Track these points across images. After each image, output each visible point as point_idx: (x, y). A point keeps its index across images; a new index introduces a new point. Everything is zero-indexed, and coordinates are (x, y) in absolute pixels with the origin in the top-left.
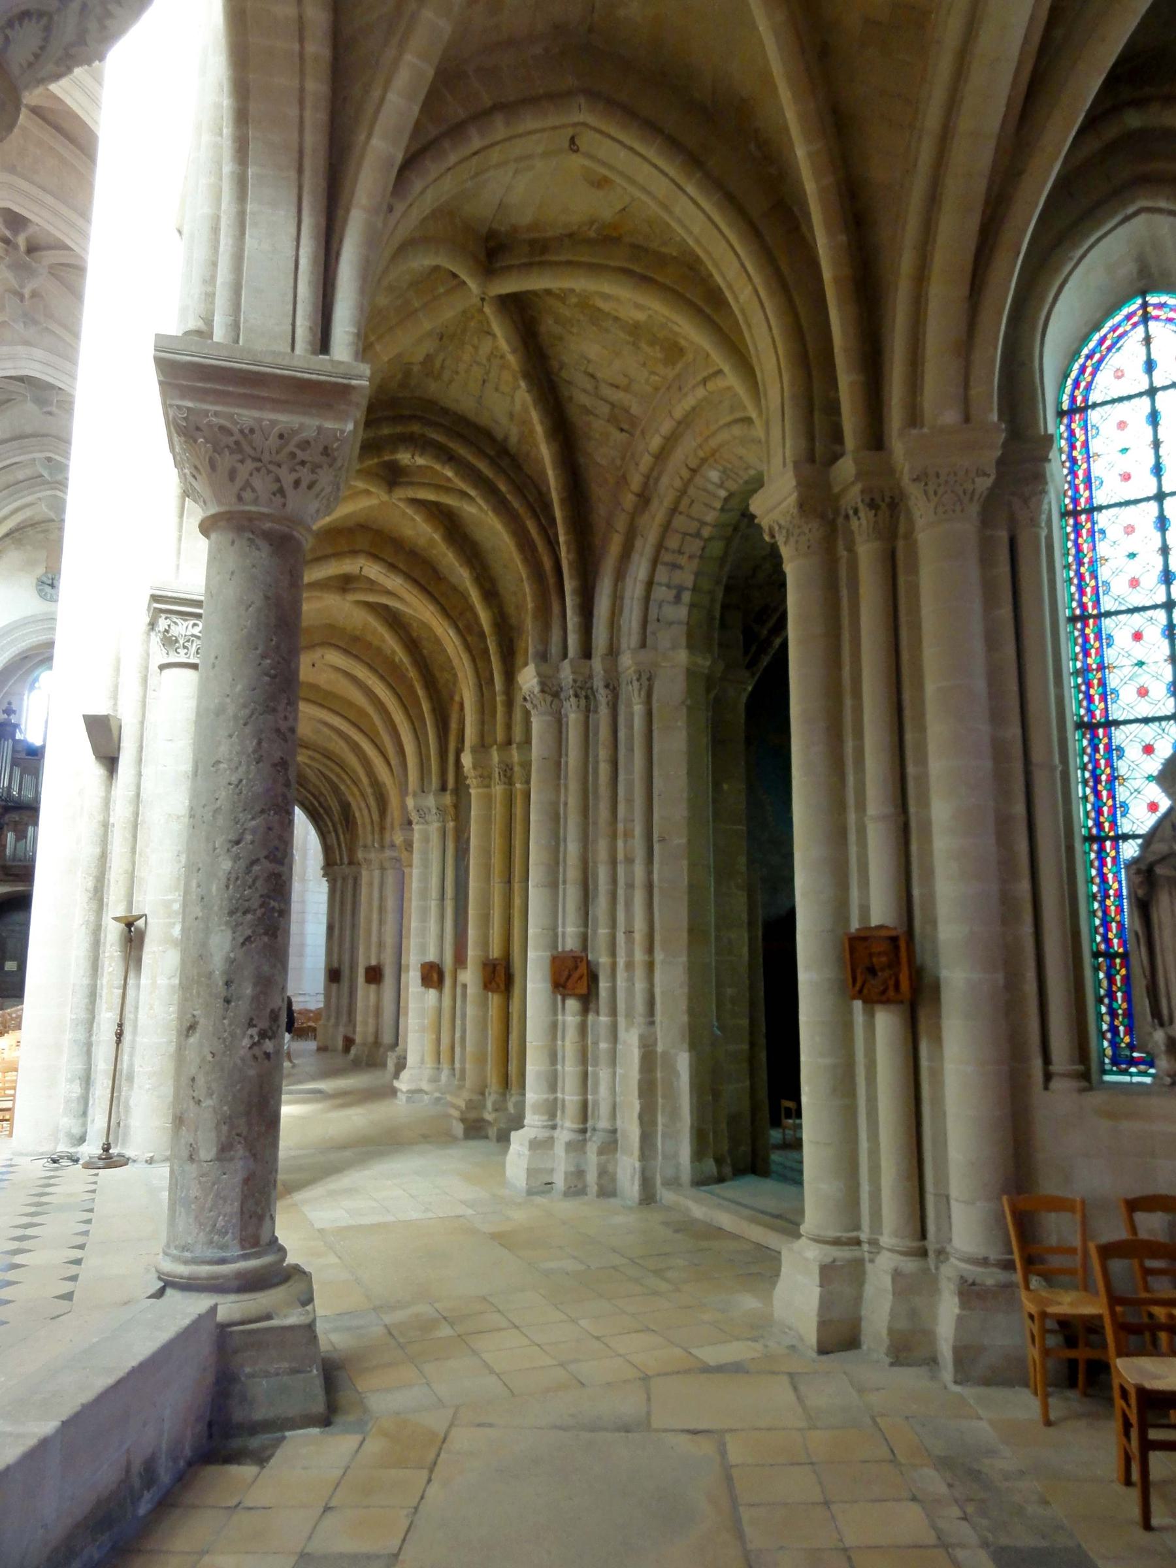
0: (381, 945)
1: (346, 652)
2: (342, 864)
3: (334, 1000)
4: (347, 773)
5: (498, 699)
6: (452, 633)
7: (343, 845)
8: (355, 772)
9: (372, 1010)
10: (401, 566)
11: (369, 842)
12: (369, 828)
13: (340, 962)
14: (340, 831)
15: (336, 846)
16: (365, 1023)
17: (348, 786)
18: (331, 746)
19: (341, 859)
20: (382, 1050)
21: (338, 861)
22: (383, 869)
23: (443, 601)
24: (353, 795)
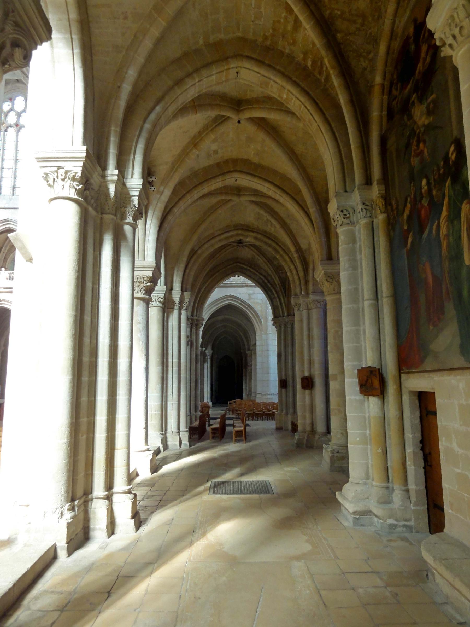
0: (311, 362)
2: (283, 316)
3: (284, 399)
4: (280, 246)
7: (283, 304)
8: (285, 245)
9: (308, 408)
12: (297, 283)
13: (286, 375)
15: (279, 305)
16: (304, 417)
18: (269, 228)
19: (283, 313)
20: (317, 437)
21: (281, 315)
22: (308, 309)
24: (285, 260)
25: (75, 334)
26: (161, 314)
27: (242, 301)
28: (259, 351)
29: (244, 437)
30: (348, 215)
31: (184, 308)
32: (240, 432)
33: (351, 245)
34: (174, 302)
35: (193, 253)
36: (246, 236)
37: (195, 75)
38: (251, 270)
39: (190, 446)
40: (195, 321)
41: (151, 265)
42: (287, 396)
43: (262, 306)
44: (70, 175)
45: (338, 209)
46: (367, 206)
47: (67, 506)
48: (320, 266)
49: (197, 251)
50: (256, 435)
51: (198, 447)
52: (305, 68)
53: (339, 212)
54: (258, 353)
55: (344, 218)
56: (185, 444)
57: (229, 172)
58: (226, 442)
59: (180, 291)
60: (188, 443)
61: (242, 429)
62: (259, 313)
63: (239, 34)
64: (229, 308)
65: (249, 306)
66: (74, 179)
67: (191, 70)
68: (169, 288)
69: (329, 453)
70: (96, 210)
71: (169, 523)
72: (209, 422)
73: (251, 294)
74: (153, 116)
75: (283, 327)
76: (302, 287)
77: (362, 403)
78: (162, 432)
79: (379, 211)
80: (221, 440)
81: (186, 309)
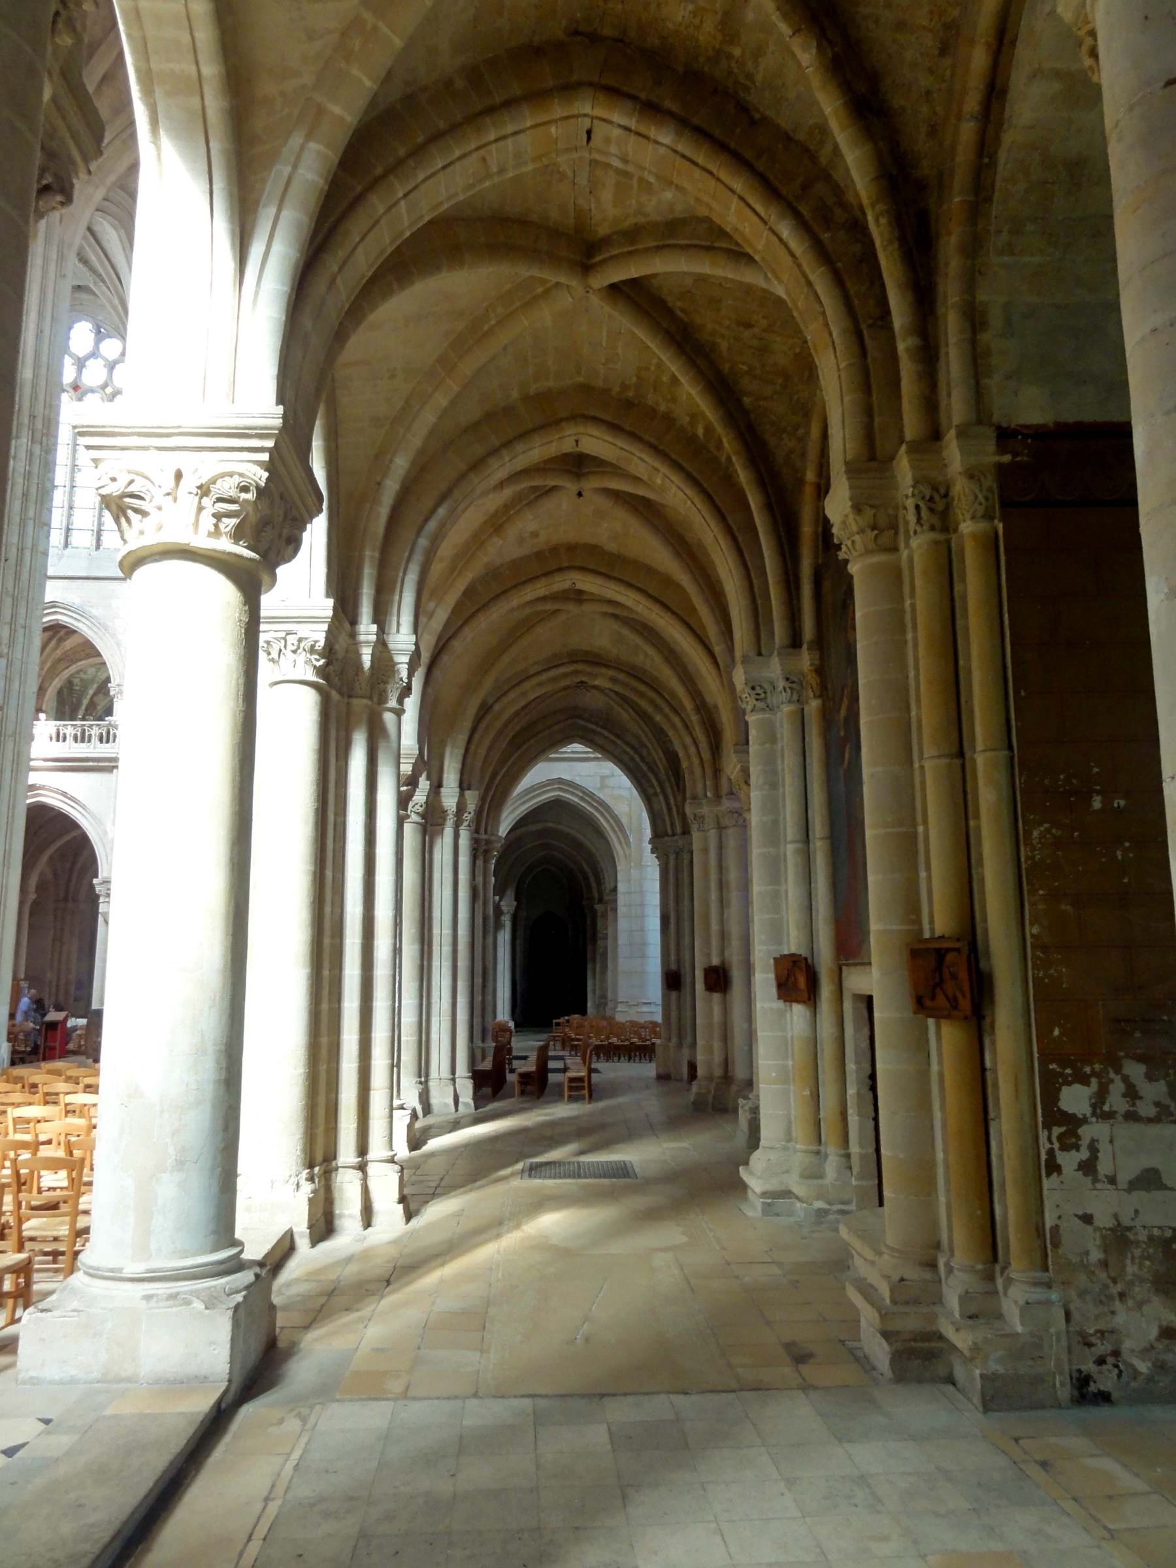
0: (724, 936)
1: (615, 428)
2: (674, 835)
3: (674, 1014)
5: (901, 347)
6: (786, 230)
7: (674, 810)
8: (673, 694)
9: (717, 1033)
10: (668, 104)
11: (700, 793)
12: (698, 771)
13: (679, 961)
14: (669, 791)
15: (665, 810)
16: (709, 1049)
17: (666, 716)
18: (639, 660)
19: (673, 825)
21: (670, 832)
22: (720, 828)
23: (760, 166)
25: (314, 902)
26: (419, 838)
27: (584, 793)
28: (625, 905)
29: (586, 1092)
30: (763, 695)
31: (466, 823)
32: (580, 1079)
33: (768, 746)
34: (444, 813)
35: (485, 709)
36: (595, 676)
37: (504, 452)
38: (606, 734)
39: (477, 1108)
40: (484, 842)
41: (410, 752)
42: (679, 1009)
43: (629, 805)
44: (306, 644)
45: (746, 684)
46: (793, 682)
47: (305, 1173)
48: (733, 756)
49: (491, 707)
50: (612, 1090)
51: (491, 1110)
52: (693, 439)
53: (748, 690)
54: (621, 910)
55: (757, 700)
56: (466, 1104)
57: (560, 570)
58: (549, 1102)
59: (458, 790)
60: (471, 1102)
61: (583, 1074)
62: (624, 821)
63: (581, 379)
64: (556, 805)
65: (602, 803)
66: (312, 650)
67: (497, 443)
68: (436, 784)
69: (748, 1113)
70: (341, 693)
71: (459, 1214)
72: (510, 1063)
73: (607, 777)
74: (432, 525)
75: (672, 857)
76: (708, 783)
77: (781, 1014)
78: (420, 1077)
79: (811, 694)
80: (539, 1098)
81: (469, 826)
